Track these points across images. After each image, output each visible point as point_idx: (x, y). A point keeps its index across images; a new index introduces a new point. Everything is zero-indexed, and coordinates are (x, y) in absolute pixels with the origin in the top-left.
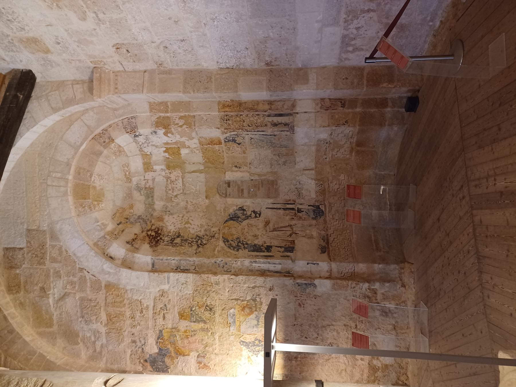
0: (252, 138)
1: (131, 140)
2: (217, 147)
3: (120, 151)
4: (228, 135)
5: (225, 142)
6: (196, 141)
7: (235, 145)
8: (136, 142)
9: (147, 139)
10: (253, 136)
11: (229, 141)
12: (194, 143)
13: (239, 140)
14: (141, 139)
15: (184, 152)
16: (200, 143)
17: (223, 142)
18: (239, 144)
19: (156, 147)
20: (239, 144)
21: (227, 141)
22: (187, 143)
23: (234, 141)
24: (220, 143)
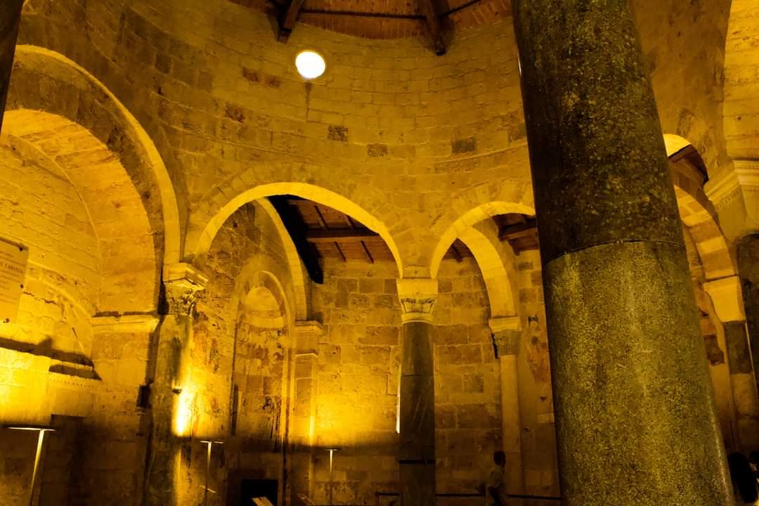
0: (269, 419)
1: (276, 327)
2: (262, 390)
3: (271, 314)
4: (274, 401)
5: (266, 398)
6: (269, 375)
7: (262, 405)
8: (274, 329)
9: (273, 338)
10: (271, 419)
11: (267, 401)
12: (266, 371)
13: (268, 408)
14: (275, 334)
15: (259, 362)
16: (265, 378)
17: (267, 395)
18: (264, 408)
19: (266, 342)
20: (264, 408)
21: (268, 400)
22: (266, 367)
23: (267, 405)
24: (265, 393)
